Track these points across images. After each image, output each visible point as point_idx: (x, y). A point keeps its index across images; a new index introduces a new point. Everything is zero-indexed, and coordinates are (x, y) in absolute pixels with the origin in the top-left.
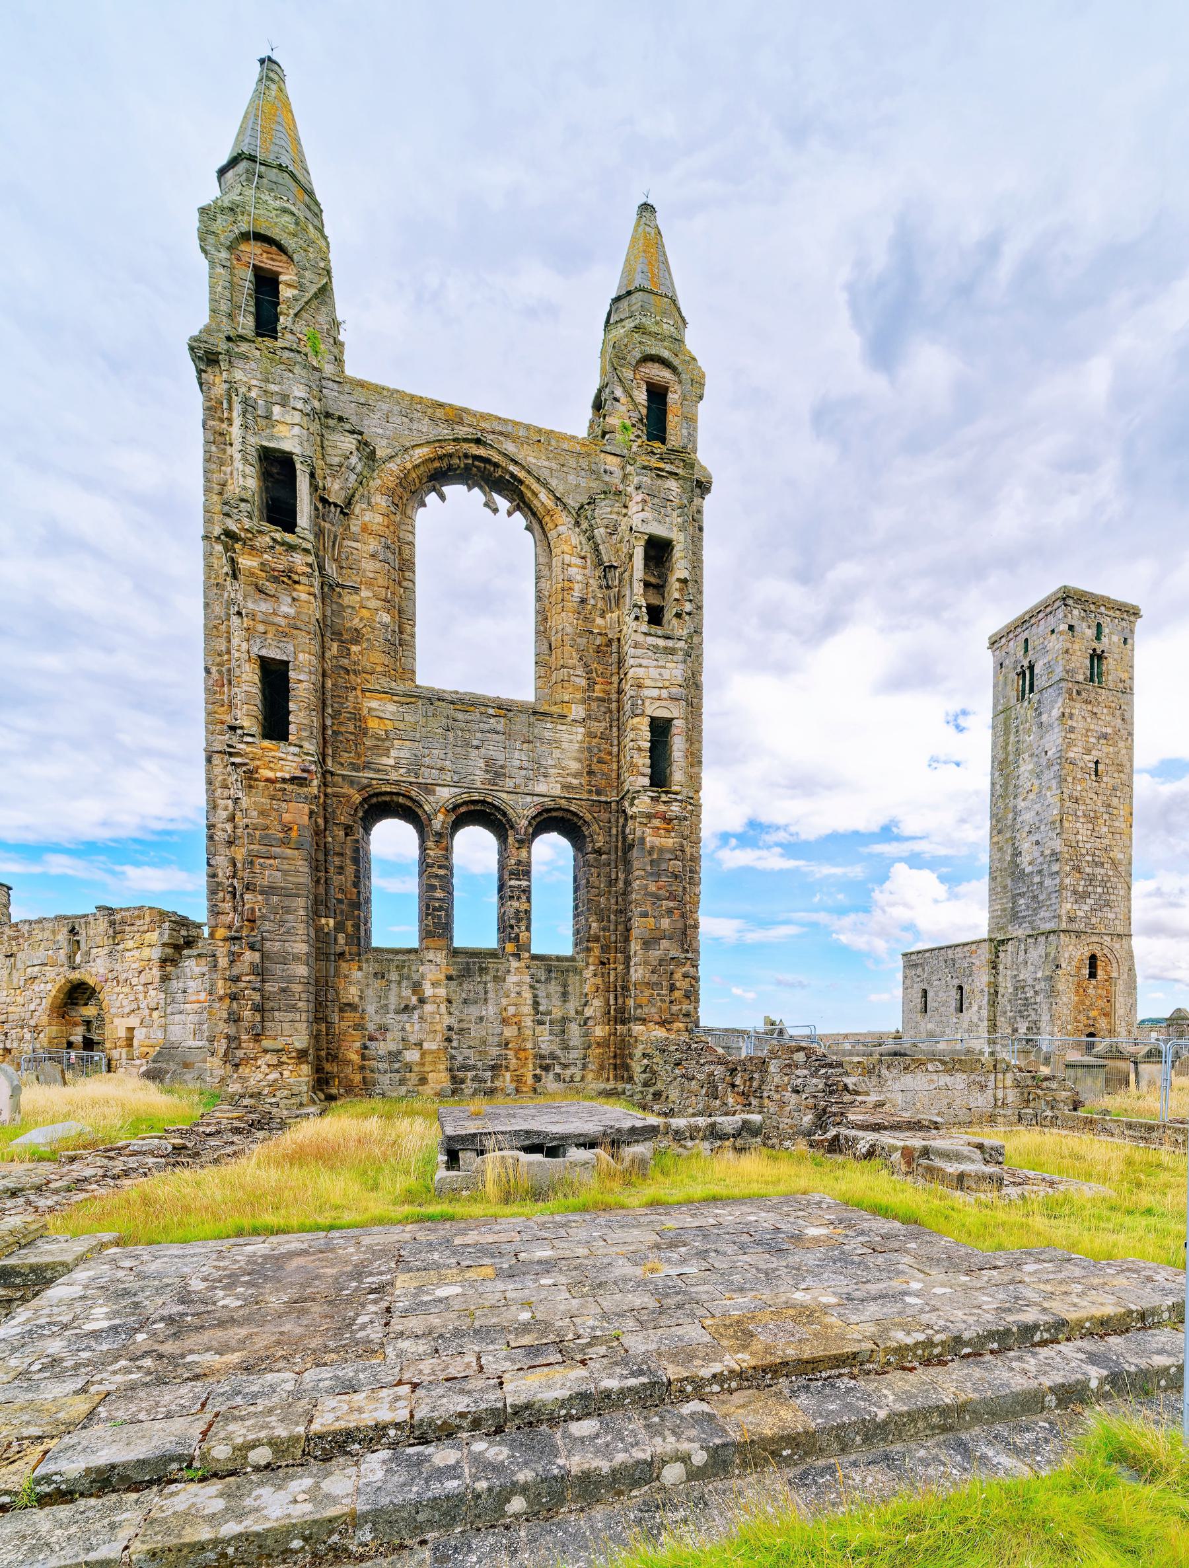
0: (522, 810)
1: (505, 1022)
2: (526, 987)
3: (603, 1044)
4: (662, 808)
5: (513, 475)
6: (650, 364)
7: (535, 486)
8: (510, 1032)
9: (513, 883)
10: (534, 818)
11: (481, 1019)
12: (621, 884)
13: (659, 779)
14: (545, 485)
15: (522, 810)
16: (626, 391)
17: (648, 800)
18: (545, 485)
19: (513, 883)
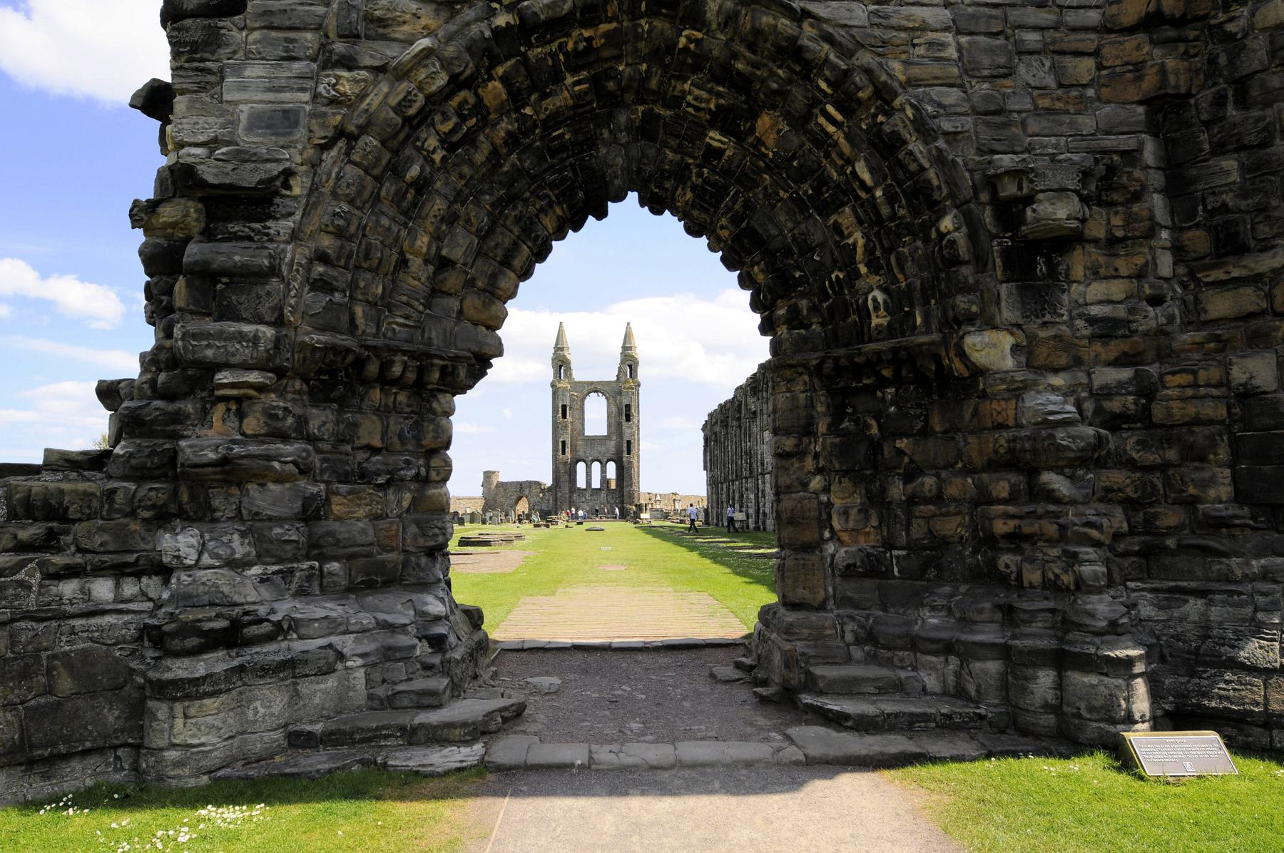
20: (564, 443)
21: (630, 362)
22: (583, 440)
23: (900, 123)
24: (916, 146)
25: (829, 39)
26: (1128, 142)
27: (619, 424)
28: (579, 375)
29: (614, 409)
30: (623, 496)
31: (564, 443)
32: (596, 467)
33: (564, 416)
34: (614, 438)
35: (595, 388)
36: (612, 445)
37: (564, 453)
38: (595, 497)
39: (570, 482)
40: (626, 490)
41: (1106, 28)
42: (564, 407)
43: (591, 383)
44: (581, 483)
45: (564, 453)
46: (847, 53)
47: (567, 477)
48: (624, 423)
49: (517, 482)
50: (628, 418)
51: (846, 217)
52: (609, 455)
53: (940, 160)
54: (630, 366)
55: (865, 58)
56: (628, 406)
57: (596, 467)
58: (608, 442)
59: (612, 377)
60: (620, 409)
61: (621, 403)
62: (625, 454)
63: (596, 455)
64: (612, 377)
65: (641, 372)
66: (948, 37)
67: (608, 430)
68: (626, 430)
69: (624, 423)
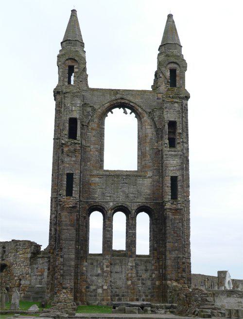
0: (133, 208)
1: (128, 279)
2: (134, 267)
3: (159, 288)
4: (175, 206)
5: (131, 105)
6: (171, 64)
7: (137, 107)
8: (129, 282)
9: (130, 231)
10: (137, 210)
11: (120, 278)
12: (163, 231)
13: (174, 196)
14: (140, 107)
15: (133, 208)
16: (163, 74)
17: (170, 204)
18: (140, 107)
19: (130, 231)
20: (70, 177)
22: (99, 176)
27: (158, 155)
29: (150, 131)
30: (165, 267)
31: (70, 177)
32: (119, 220)
34: (150, 174)
36: (146, 185)
37: (69, 193)
38: (117, 268)
39: (77, 241)
40: (171, 257)
42: (73, 122)
43: (116, 92)
44: (95, 246)
45: (69, 193)
47: (73, 232)
48: (167, 150)
50: (172, 143)
52: (141, 200)
54: (173, 72)
56: (172, 125)
57: (119, 220)
58: (140, 181)
60: (158, 131)
61: (161, 117)
62: (168, 197)
63: (121, 199)
65: (191, 82)
67: (141, 156)
68: (172, 164)
69: (167, 150)
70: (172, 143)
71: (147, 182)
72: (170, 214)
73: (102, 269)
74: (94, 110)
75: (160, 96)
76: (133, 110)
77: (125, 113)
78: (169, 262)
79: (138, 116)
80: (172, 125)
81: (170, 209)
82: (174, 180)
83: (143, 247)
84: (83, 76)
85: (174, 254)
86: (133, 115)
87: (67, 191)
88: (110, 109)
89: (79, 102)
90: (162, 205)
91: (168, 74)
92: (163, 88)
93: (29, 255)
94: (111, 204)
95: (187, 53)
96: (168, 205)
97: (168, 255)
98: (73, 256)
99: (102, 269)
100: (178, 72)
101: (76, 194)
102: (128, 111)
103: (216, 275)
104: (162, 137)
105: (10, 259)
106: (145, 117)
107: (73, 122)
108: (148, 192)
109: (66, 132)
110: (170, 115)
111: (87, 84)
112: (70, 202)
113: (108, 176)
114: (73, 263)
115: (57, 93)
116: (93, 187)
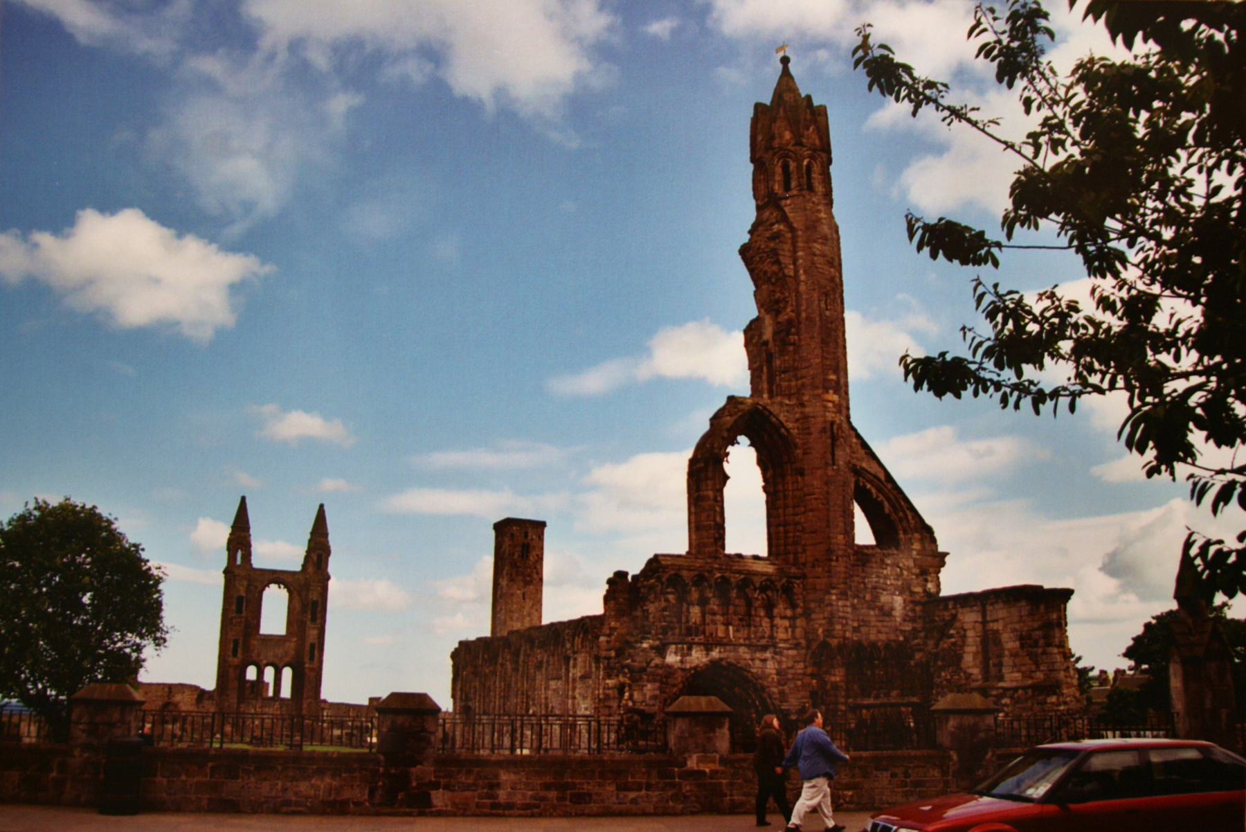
21: (320, 552)
23: (765, 695)
24: (768, 700)
25: (753, 676)
26: (806, 700)
28: (257, 563)
29: (298, 606)
31: (236, 643)
33: (239, 611)
35: (277, 577)
36: (291, 645)
37: (235, 654)
41: (804, 674)
43: (274, 572)
45: (235, 654)
46: (756, 679)
49: (164, 685)
51: (753, 710)
52: (287, 659)
53: (773, 704)
54: (319, 557)
55: (760, 681)
58: (287, 644)
59: (296, 565)
63: (271, 659)
64: (296, 565)
65: (333, 566)
66: (775, 677)
70: (314, 620)
71: (292, 645)
72: (307, 670)
73: (255, 709)
74: (256, 587)
75: (308, 576)
76: (286, 587)
77: (280, 587)
78: (305, 706)
79: (289, 591)
80: (315, 604)
81: (308, 668)
82: (312, 646)
83: (286, 692)
84: (247, 556)
85: (309, 701)
86: (286, 590)
87: (233, 652)
88: (268, 585)
89: (245, 583)
90: (304, 664)
91: (315, 558)
92: (311, 570)
93: (195, 696)
94: (265, 662)
95: (335, 539)
96: (307, 665)
97: (304, 701)
98: (236, 701)
99: (255, 709)
100: (323, 557)
101: (239, 655)
102: (282, 586)
103: (366, 703)
104: (306, 612)
105: (178, 698)
106: (295, 594)
107: (240, 599)
108: (293, 652)
109: (234, 607)
110: (314, 596)
111: (251, 565)
112: (236, 661)
113: (263, 640)
114: (235, 706)
115: (226, 572)
116: (251, 648)
